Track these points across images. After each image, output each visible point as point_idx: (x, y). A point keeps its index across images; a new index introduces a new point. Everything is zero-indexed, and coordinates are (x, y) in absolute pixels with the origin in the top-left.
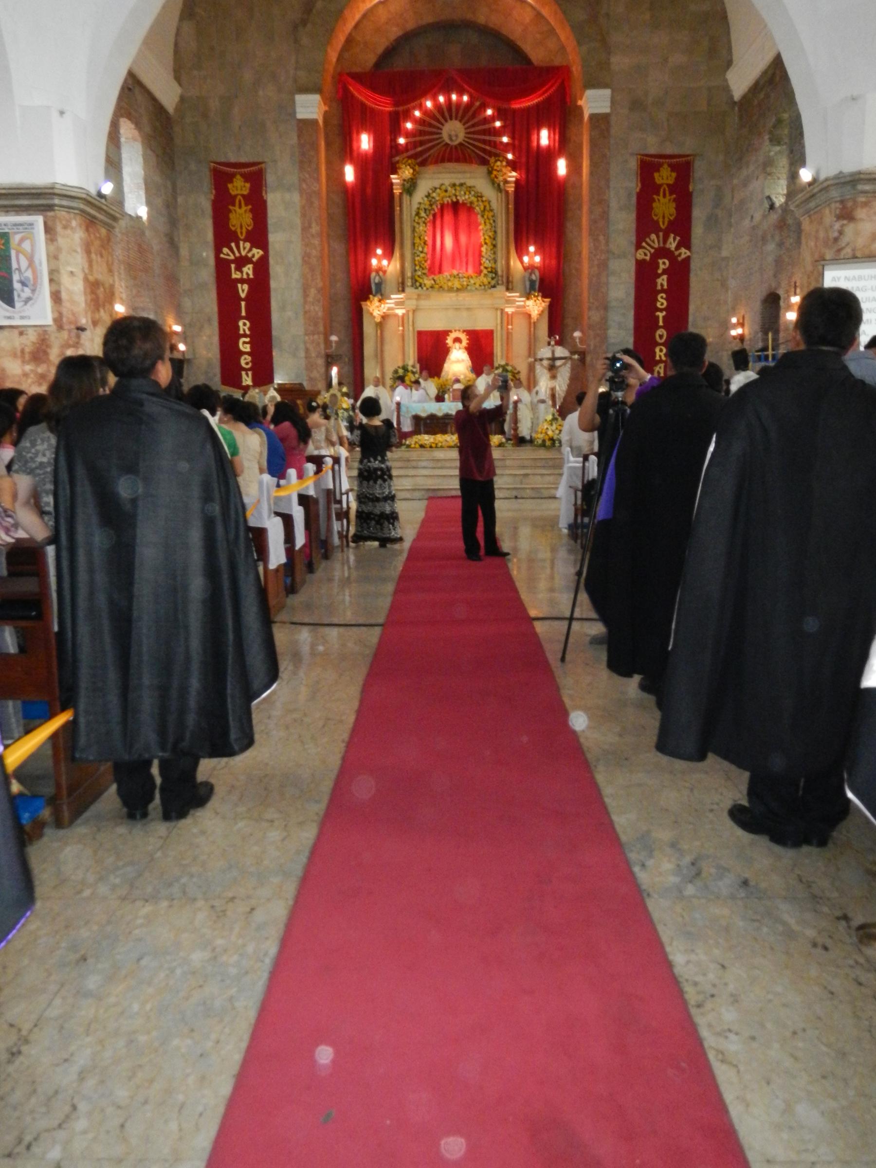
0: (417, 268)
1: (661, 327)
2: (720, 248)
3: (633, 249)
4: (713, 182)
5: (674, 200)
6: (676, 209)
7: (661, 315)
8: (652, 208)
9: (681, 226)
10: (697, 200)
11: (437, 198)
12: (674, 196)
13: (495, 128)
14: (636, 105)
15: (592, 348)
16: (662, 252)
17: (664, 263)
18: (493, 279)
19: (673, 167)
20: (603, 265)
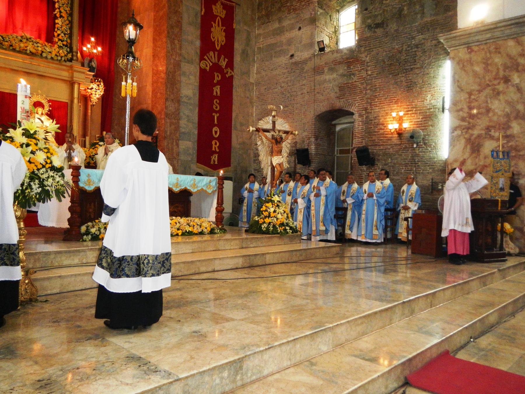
1: (215, 125)
2: (249, 76)
3: (198, 60)
4: (245, 28)
6: (226, 37)
7: (216, 116)
9: (228, 50)
10: (237, 37)
12: (224, 28)
15: (168, 133)
16: (216, 67)
17: (218, 76)
18: (68, 53)
19: (225, 7)
20: (177, 65)
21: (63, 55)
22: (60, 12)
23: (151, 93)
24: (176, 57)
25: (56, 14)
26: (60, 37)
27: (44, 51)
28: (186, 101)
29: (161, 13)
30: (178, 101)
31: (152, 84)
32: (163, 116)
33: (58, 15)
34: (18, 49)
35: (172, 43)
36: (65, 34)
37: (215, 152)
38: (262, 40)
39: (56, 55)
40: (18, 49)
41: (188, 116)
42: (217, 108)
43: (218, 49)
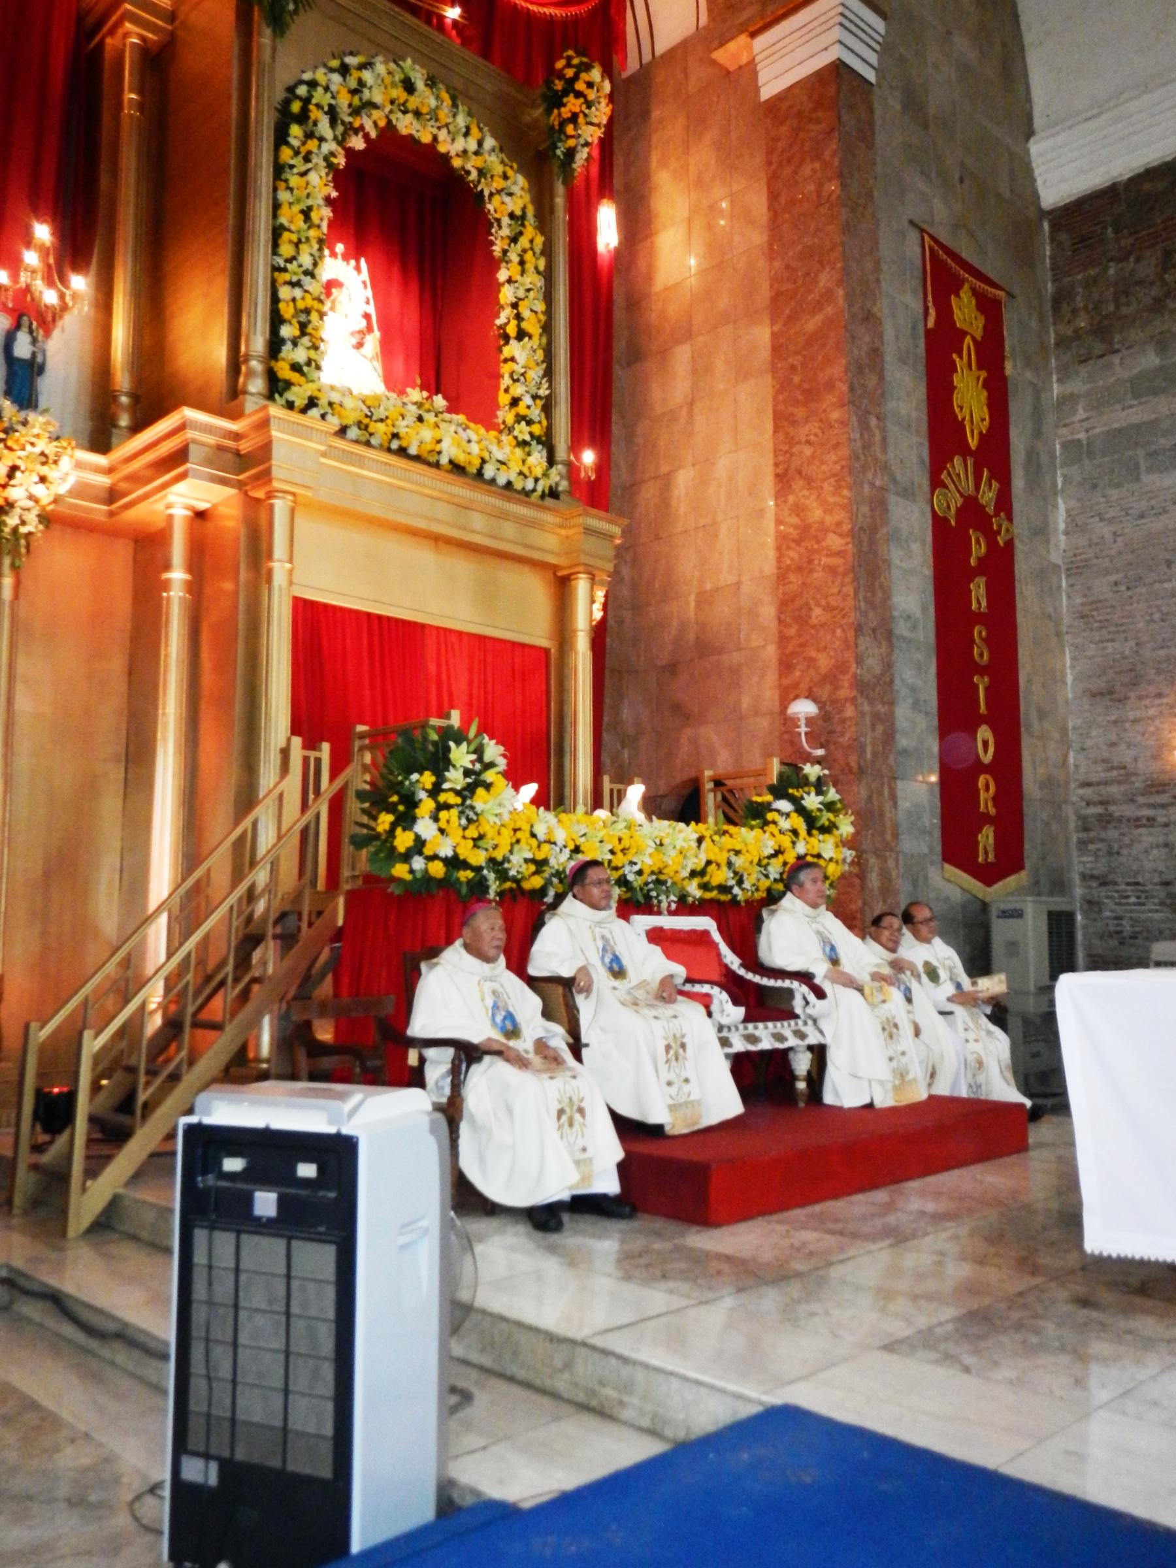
0: (286, 331)
1: (980, 720)
2: (1048, 542)
4: (1029, 375)
5: (986, 385)
6: (991, 405)
7: (982, 684)
8: (953, 388)
9: (994, 455)
11: (378, 98)
13: (442, 18)
14: (913, 104)
15: (869, 756)
16: (971, 510)
17: (978, 542)
20: (880, 505)
21: (538, 472)
22: (519, 317)
23: (768, 612)
24: (875, 475)
25: (500, 327)
26: (521, 409)
27: (486, 456)
28: (905, 633)
29: (812, 324)
30: (885, 632)
31: (782, 575)
32: (844, 693)
33: (512, 330)
34: (413, 451)
35: (864, 426)
36: (535, 397)
37: (986, 819)
38: (1081, 414)
39: (521, 473)
40: (413, 451)
41: (913, 689)
42: (981, 655)
43: (973, 443)
